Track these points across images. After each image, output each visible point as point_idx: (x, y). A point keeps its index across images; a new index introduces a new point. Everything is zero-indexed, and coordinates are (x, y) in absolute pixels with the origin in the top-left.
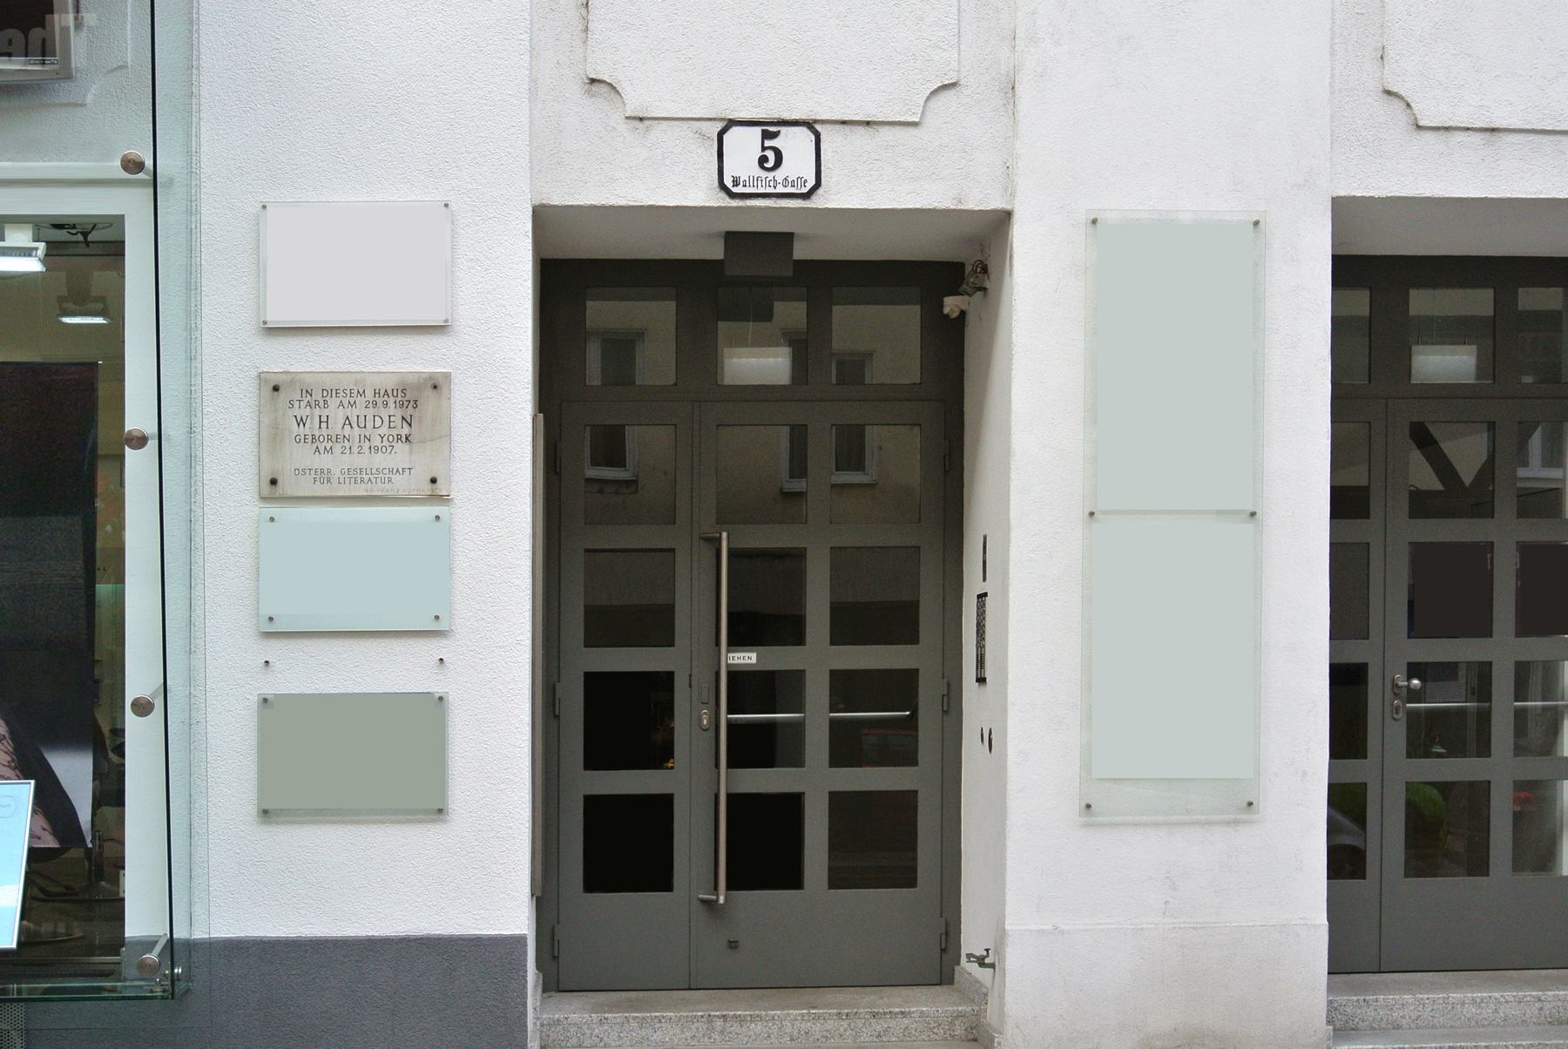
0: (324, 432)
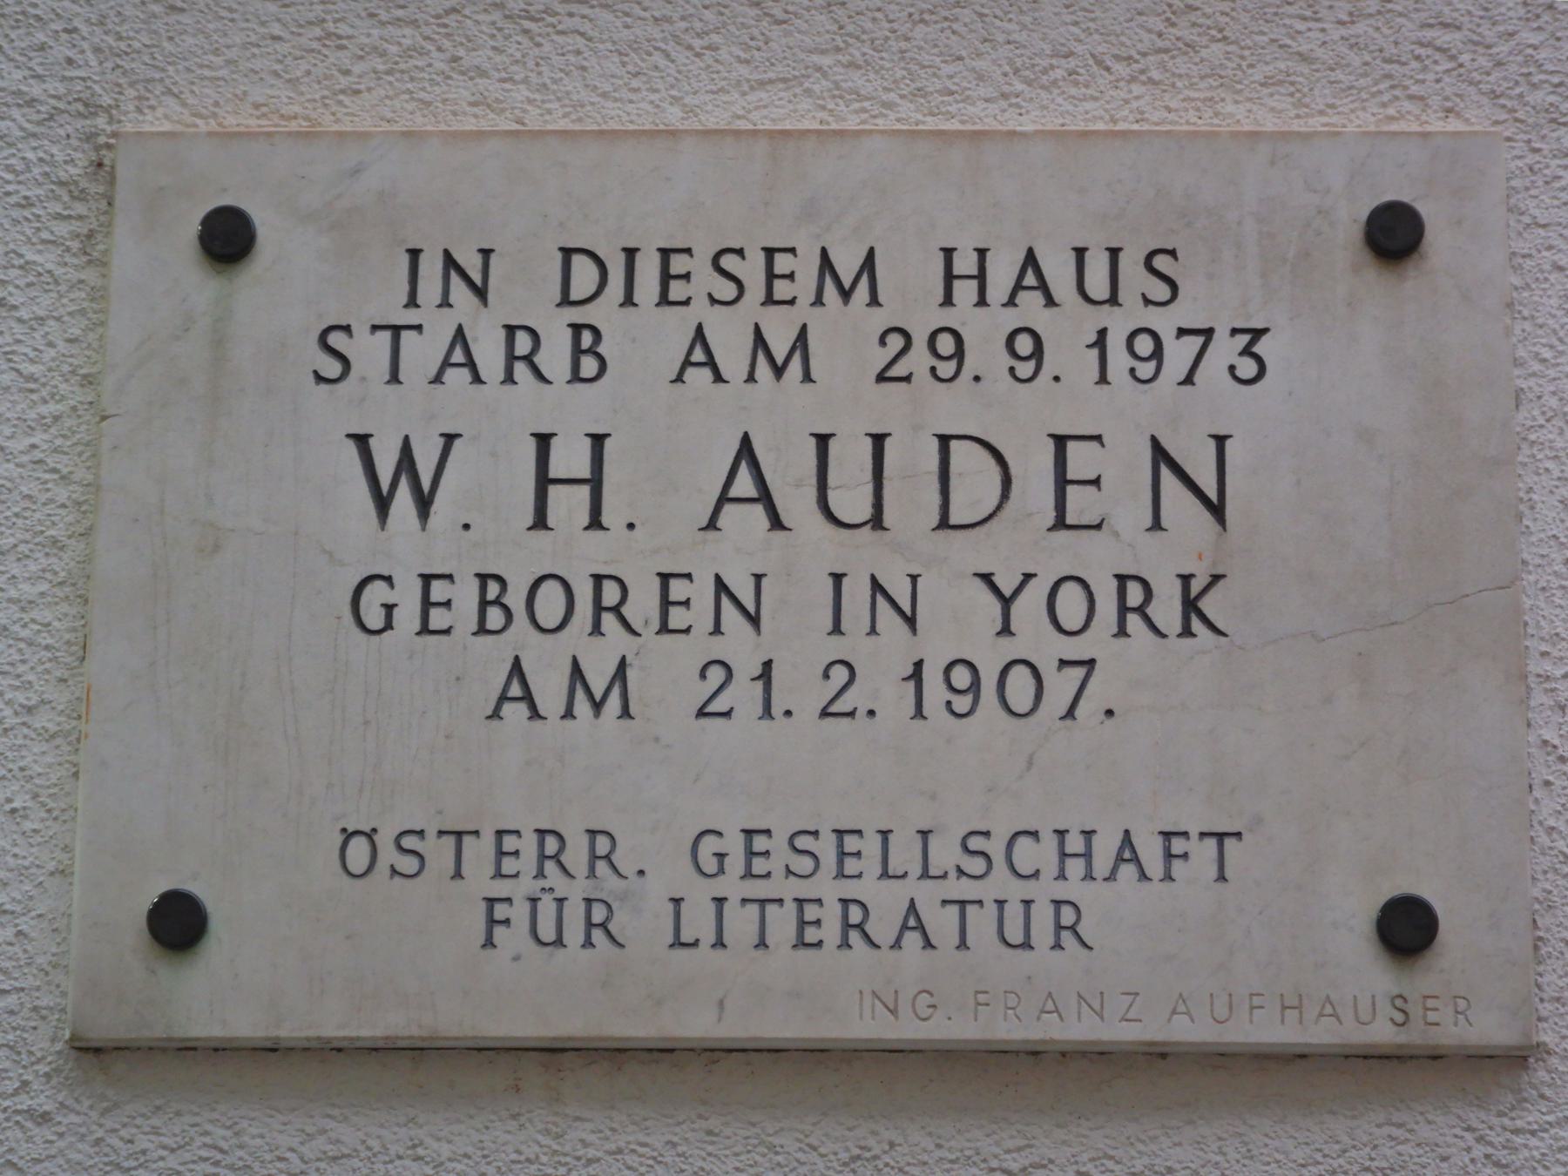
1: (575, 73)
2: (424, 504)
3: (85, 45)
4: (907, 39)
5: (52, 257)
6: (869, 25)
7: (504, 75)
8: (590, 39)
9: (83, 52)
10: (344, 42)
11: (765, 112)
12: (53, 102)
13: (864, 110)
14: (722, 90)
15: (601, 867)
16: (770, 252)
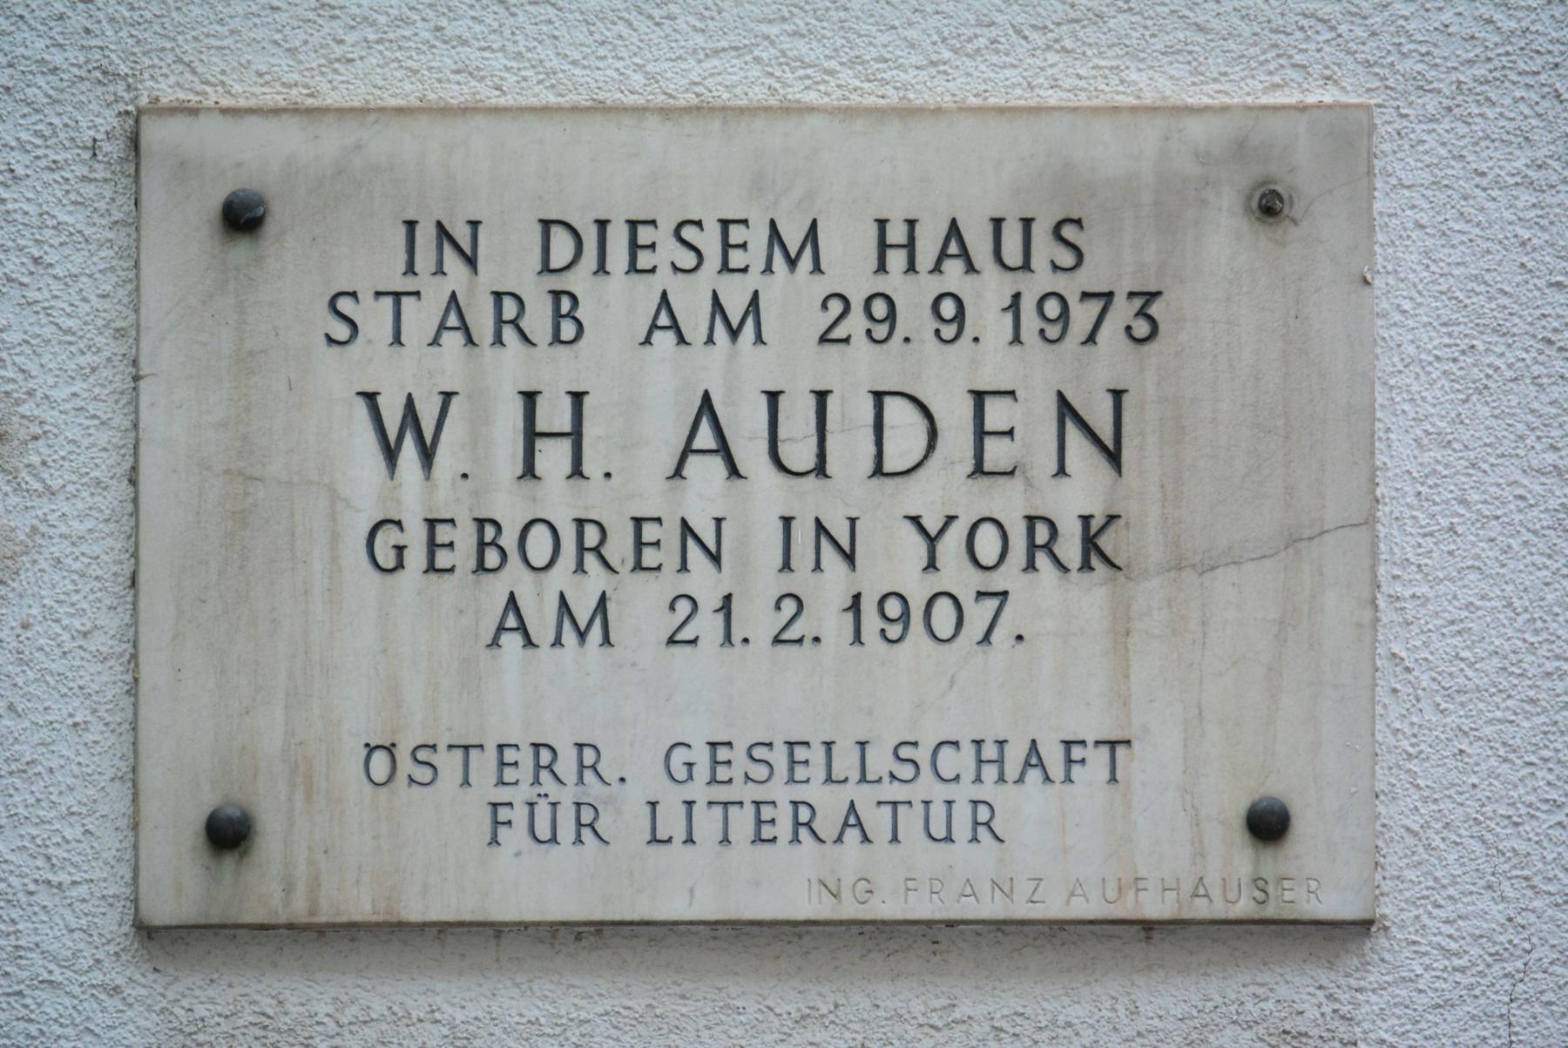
0: (558, 499)
1: (548, 42)
2: (427, 455)
3: (101, 15)
4: (846, 9)
5: (81, 217)
7: (483, 44)
8: (560, 9)
9: (99, 22)
10: (337, 12)
11: (719, 79)
12: (75, 71)
13: (808, 77)
14: (680, 58)
15: (589, 776)
16: (725, 224)
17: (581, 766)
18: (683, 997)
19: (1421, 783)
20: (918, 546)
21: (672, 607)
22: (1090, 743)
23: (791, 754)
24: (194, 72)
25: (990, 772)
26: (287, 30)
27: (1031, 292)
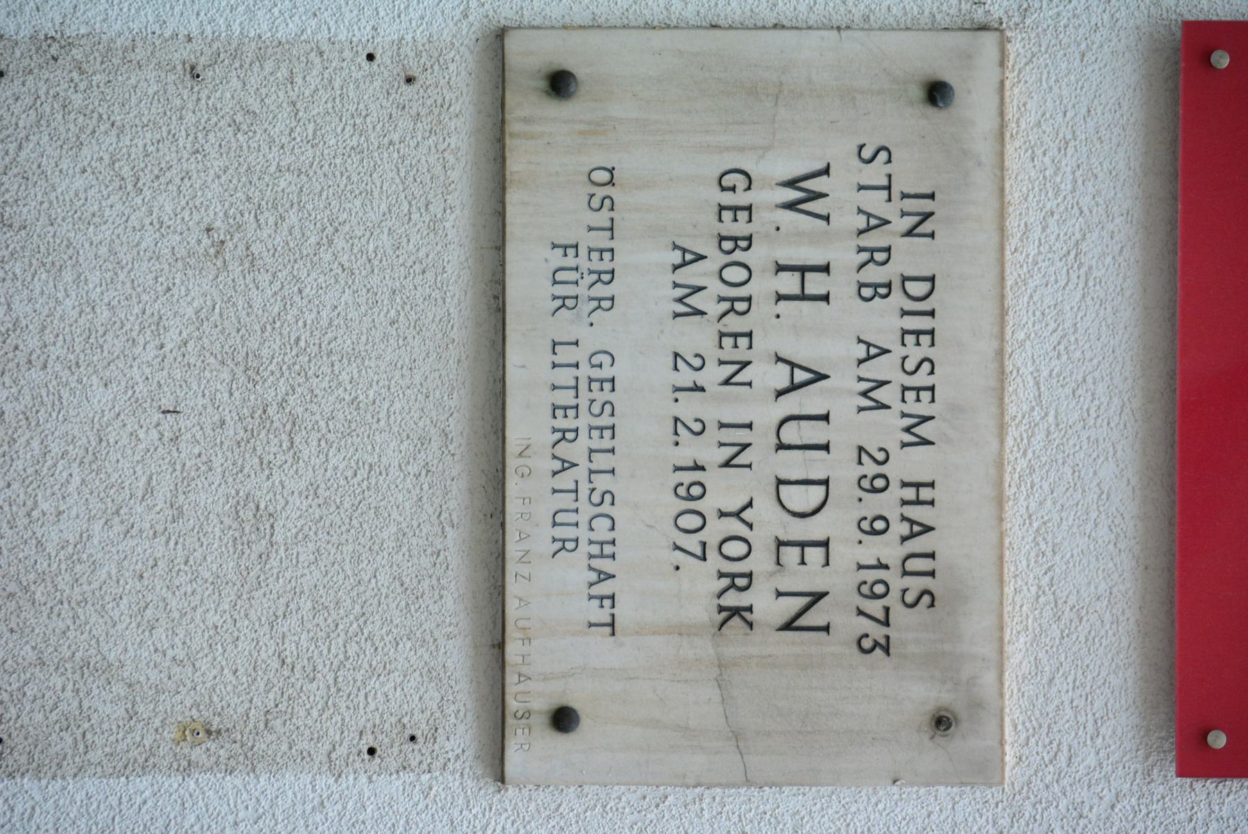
0: (763, 286)
2: (791, 206)
6: (1071, 442)
15: (595, 304)
16: (932, 389)
17: (600, 300)
18: (459, 361)
19: (588, 813)
20: (734, 506)
21: (697, 355)
22: (613, 611)
23: (607, 428)
24: (1026, 64)
25: (595, 549)
26: (1051, 121)
27: (889, 576)
